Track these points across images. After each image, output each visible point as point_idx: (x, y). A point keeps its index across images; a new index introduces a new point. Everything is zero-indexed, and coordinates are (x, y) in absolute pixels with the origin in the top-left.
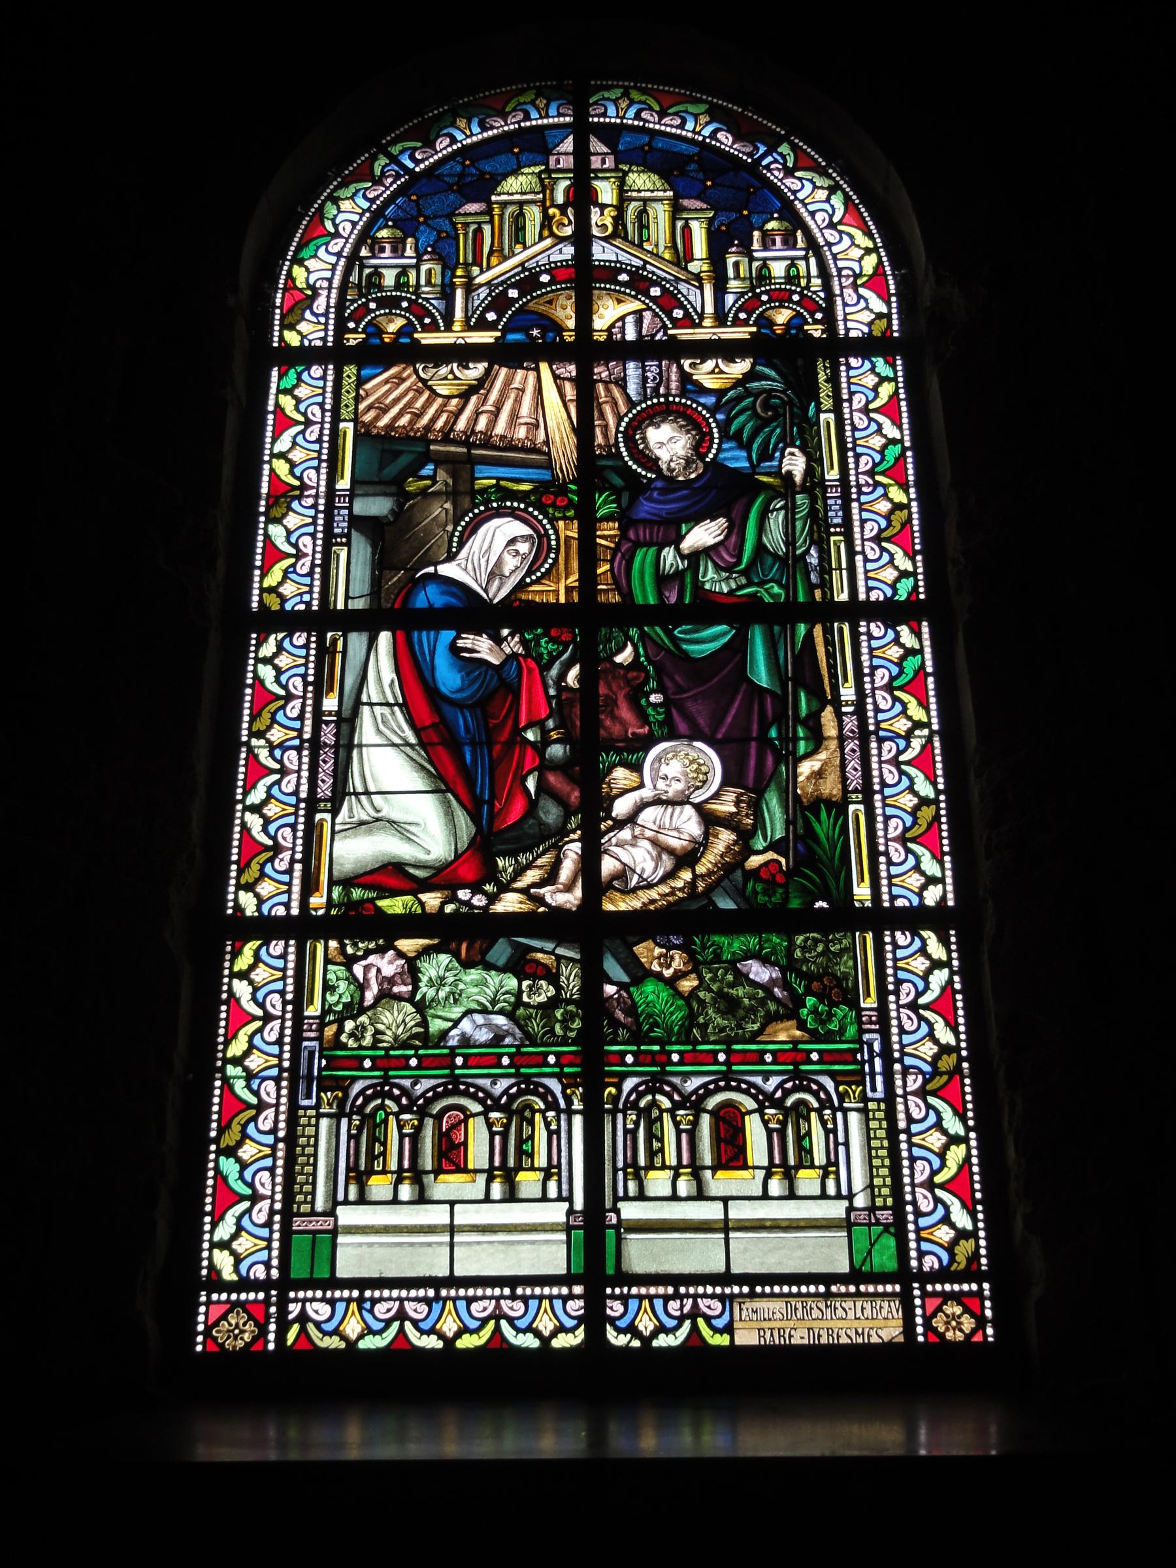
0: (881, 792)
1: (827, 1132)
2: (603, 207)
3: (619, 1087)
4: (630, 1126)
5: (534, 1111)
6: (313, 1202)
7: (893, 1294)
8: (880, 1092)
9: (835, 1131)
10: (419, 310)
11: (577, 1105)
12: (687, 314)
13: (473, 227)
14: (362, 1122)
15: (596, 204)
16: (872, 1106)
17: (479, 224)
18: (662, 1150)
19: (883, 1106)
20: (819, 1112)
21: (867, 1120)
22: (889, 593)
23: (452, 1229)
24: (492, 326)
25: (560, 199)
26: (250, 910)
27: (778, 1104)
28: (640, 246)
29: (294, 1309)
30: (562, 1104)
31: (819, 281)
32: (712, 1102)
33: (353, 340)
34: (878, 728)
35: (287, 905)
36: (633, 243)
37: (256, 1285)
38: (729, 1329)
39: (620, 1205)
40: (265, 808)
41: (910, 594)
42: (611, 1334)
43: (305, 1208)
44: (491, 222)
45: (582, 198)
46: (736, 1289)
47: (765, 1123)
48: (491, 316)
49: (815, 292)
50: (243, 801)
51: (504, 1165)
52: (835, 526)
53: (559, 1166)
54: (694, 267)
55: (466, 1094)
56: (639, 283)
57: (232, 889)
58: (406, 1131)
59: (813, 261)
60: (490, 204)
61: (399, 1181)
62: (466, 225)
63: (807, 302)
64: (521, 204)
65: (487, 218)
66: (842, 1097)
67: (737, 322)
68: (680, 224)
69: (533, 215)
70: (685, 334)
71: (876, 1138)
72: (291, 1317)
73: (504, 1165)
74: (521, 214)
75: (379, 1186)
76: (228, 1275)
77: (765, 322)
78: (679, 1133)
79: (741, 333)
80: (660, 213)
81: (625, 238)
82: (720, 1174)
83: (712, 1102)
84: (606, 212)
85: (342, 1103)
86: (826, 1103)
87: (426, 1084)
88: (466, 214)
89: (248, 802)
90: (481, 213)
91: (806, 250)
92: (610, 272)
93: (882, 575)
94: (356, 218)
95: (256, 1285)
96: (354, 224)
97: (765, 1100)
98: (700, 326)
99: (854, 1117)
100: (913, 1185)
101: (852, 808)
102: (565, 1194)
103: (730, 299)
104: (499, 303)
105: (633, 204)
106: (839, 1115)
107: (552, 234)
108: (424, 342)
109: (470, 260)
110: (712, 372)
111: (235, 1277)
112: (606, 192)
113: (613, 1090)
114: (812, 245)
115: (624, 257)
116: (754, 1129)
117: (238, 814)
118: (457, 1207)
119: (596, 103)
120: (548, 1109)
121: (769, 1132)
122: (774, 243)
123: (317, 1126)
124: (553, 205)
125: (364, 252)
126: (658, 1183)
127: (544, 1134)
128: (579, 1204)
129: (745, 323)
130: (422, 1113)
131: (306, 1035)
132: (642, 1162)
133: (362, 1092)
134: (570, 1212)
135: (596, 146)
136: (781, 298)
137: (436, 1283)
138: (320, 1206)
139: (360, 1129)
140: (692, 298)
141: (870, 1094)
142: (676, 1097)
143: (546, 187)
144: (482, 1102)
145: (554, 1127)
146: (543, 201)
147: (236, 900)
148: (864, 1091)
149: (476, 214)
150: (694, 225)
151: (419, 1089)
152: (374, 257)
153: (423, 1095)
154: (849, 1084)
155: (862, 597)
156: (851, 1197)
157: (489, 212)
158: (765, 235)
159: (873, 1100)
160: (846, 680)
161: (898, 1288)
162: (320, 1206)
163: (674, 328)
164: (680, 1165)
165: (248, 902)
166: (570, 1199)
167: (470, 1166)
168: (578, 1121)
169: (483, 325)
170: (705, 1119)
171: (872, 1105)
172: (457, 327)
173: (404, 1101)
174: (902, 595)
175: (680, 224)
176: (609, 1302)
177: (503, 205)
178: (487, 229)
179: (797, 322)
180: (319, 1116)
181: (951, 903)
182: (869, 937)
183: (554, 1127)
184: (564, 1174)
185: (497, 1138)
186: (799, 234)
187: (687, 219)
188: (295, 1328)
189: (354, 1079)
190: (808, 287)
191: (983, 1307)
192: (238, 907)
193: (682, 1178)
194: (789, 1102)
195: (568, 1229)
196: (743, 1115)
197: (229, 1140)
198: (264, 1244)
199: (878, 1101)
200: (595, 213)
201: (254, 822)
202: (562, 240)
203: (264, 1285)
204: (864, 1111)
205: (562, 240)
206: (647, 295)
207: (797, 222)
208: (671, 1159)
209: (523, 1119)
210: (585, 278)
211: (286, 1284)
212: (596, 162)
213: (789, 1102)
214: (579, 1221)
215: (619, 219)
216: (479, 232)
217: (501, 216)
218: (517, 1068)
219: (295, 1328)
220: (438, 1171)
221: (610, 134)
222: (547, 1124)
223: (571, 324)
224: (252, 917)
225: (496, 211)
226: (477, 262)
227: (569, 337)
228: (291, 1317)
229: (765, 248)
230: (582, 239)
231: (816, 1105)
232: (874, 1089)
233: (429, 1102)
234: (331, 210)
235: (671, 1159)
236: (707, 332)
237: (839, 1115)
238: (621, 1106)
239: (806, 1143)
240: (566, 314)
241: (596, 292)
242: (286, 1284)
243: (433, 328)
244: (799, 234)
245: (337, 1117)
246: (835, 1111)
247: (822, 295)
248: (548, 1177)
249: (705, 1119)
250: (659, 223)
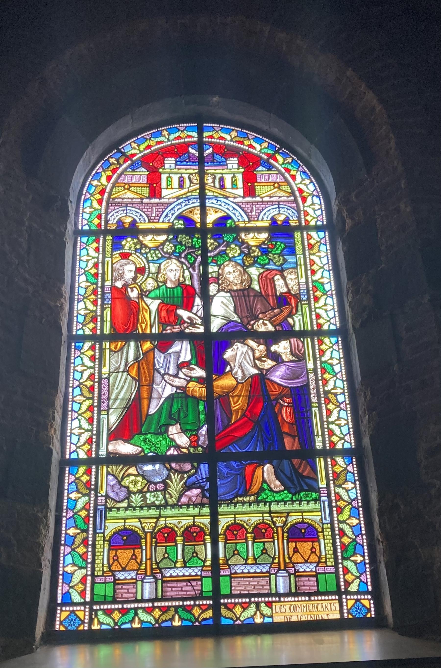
7: (335, 600)
8: (328, 521)
19: (329, 526)
38: (272, 617)
46: (274, 599)
52: (304, 301)
71: (327, 539)
141: (324, 521)
160: (309, 360)
161: (337, 597)
171: (325, 526)
182: (322, 460)
199: (327, 524)
223: (199, 220)
227: (198, 225)
232: (326, 520)
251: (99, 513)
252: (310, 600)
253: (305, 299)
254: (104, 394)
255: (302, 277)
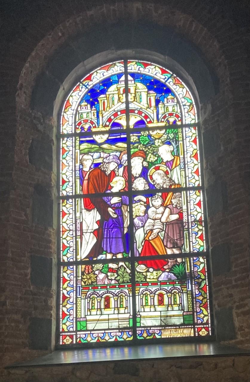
0: (191, 228)
1: (180, 297)
2: (131, 94)
3: (139, 290)
4: (142, 298)
5: (123, 296)
6: (81, 316)
9: (181, 297)
10: (92, 123)
11: (131, 295)
12: (150, 120)
13: (103, 101)
14: (90, 300)
15: (130, 93)
16: (189, 292)
17: (104, 100)
18: (147, 302)
20: (178, 293)
21: (187, 295)
22: (194, 185)
23: (108, 320)
24: (108, 126)
25: (122, 92)
26: (66, 261)
27: (171, 293)
28: (140, 103)
29: (78, 336)
30: (128, 295)
31: (180, 110)
32: (157, 293)
33: (78, 131)
34: (191, 214)
35: (73, 259)
36: (138, 103)
37: (71, 332)
39: (140, 313)
40: (67, 239)
41: (198, 185)
42: (138, 337)
43: (80, 317)
44: (107, 99)
45: (127, 91)
47: (168, 296)
48: (108, 123)
49: (179, 113)
50: (62, 237)
51: (117, 307)
53: (128, 307)
54: (152, 109)
55: (110, 293)
56: (140, 113)
57: (62, 256)
58: (98, 301)
59: (178, 105)
60: (106, 95)
61: (97, 311)
62: (101, 100)
63: (177, 116)
64: (113, 94)
65: (106, 98)
66: (182, 290)
67: (161, 122)
68: (149, 97)
69: (116, 97)
70: (150, 125)
72: (78, 337)
73: (117, 307)
74: (113, 97)
75: (94, 312)
76: (66, 330)
77: (168, 121)
78: (151, 299)
79: (163, 124)
80: (144, 95)
81: (137, 102)
82: (160, 306)
83: (157, 293)
84: (132, 94)
85: (86, 296)
86: (179, 292)
87: (102, 292)
88: (101, 98)
89: (63, 237)
90: (104, 97)
91: (177, 103)
92: (133, 111)
93: (192, 181)
94: (77, 100)
95: (71, 332)
96: (77, 102)
97: (168, 292)
98: (153, 123)
99: (185, 294)
100: (196, 307)
101: (185, 232)
102: (129, 312)
103: (160, 116)
104: (110, 120)
105: (138, 93)
106: (182, 294)
107: (120, 101)
108: (93, 131)
109: (103, 109)
110: (156, 134)
111: (67, 331)
112: (132, 90)
113: (138, 291)
114: (178, 102)
115: (136, 107)
116: (165, 297)
117: (61, 240)
118: (109, 315)
119: (129, 66)
120: (126, 295)
121: (169, 298)
122: (169, 101)
123: (81, 301)
124: (120, 94)
125: (79, 109)
126: (147, 309)
127: (125, 301)
128: (132, 314)
129: (163, 122)
130: (101, 297)
131: (78, 283)
132: (144, 304)
133: (90, 294)
134: (130, 315)
135: (130, 78)
136: (171, 115)
137: (105, 330)
138: (83, 316)
139: (89, 301)
140: (151, 116)
141: (188, 290)
142: (151, 292)
143: (118, 90)
144: (113, 295)
145: (127, 299)
146: (118, 93)
147: (63, 258)
148: (187, 289)
149: (103, 97)
150: (151, 97)
151: (100, 293)
152: (81, 110)
153: (101, 294)
154: (184, 288)
155: (188, 186)
156: (184, 310)
157: (106, 97)
158: (167, 99)
159: (189, 291)
162: (83, 316)
163: (148, 123)
164: (151, 305)
165: (65, 259)
166: (130, 313)
167: (111, 307)
168: (131, 298)
169: (106, 126)
170: (156, 296)
172: (101, 126)
173: (98, 295)
174: (196, 185)
175: (149, 97)
176: (138, 331)
177: (109, 95)
178: (106, 101)
179: (175, 122)
180: (81, 299)
181: (205, 251)
183: (127, 299)
184: (129, 308)
185: (116, 302)
186: (175, 98)
187: (150, 96)
188: (79, 339)
189: (88, 292)
190: (177, 112)
191: (209, 329)
192: (63, 260)
193: (152, 308)
194: (173, 292)
195: (129, 318)
196: (163, 295)
197: (64, 304)
198: (72, 324)
200: (129, 95)
201: (65, 242)
202: (123, 103)
203: (73, 332)
204: (187, 293)
205: (123, 103)
206: (141, 116)
207: (174, 95)
208: (149, 304)
209: (121, 298)
210: (127, 112)
211: (77, 331)
212: (129, 82)
213: (173, 292)
214: (131, 317)
215: (135, 97)
216: (104, 103)
217: (109, 97)
218: (120, 288)
219: (79, 339)
220: (104, 309)
221: (133, 75)
222: (125, 299)
224: (67, 262)
225: (108, 97)
226: (104, 109)
228: (78, 337)
229: (167, 103)
230: (127, 103)
231: (178, 292)
232: (189, 289)
233: (103, 295)
234: (71, 98)
235: (149, 304)
236: (155, 124)
237: (182, 294)
238: (140, 294)
239: (175, 300)
240: (123, 122)
241: (130, 116)
242: (77, 331)
243: (95, 127)
244: (175, 98)
245: (85, 299)
246: (181, 293)
247: (180, 114)
248: (126, 308)
249: (156, 296)
250: (143, 98)
251: (78, 288)
252: (179, 328)
253: (183, 168)
254: (78, 227)
255: (181, 154)
